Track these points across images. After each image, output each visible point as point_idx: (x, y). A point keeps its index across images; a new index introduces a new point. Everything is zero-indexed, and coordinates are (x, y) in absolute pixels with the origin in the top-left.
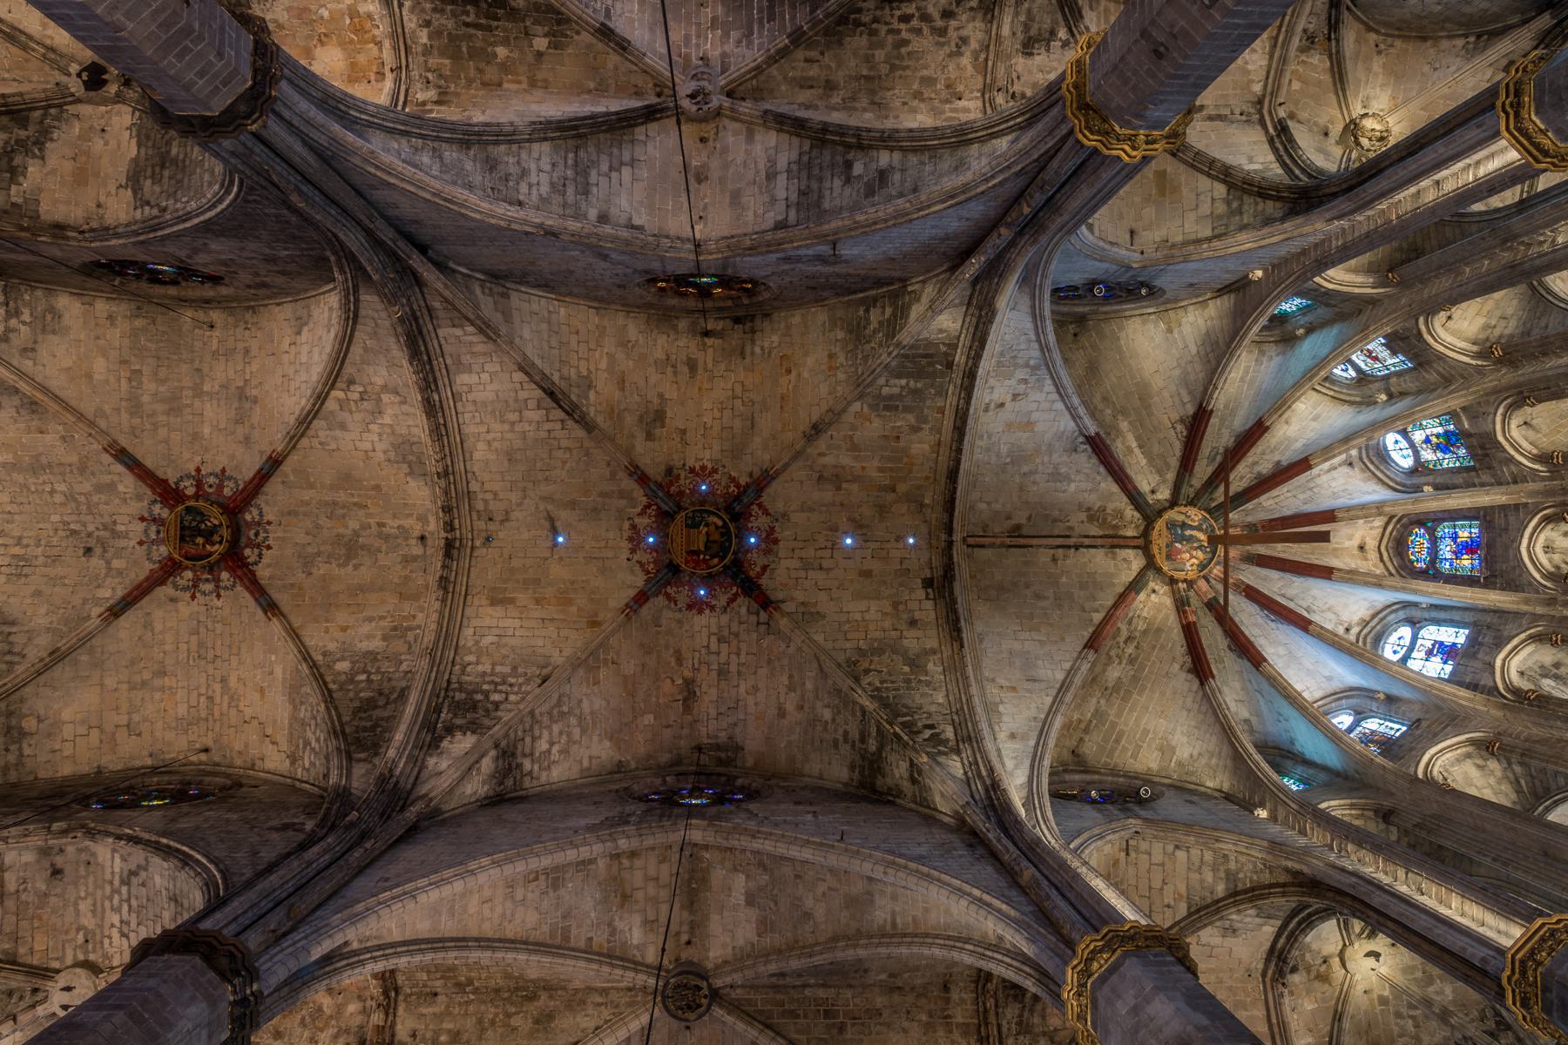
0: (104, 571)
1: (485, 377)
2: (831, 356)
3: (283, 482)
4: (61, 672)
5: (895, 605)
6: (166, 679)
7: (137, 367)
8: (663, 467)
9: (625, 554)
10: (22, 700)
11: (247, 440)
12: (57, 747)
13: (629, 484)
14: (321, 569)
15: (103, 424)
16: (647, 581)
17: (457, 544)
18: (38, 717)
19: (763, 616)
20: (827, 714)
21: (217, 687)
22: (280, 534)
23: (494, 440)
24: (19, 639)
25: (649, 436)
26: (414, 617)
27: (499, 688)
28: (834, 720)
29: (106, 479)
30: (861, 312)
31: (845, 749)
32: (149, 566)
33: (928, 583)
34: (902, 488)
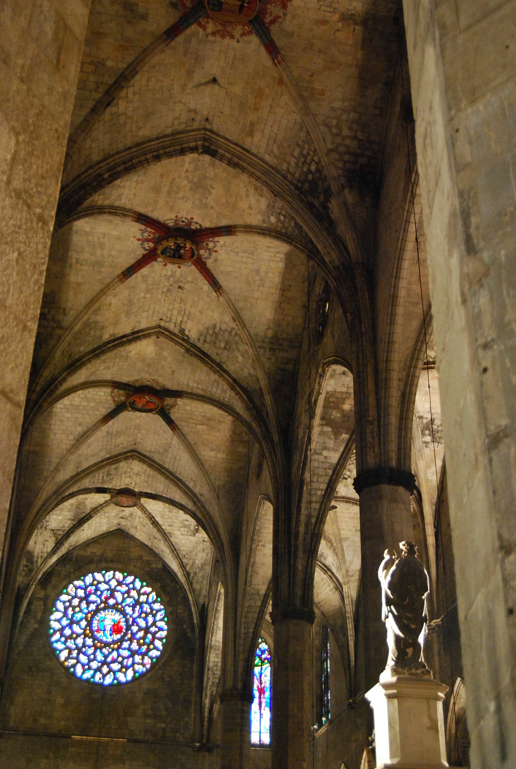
0: (193, 285)
1: (93, 145)
3: (152, 212)
4: (246, 315)
6: (261, 270)
7: (74, 260)
8: (170, 10)
9: (234, 43)
10: (257, 335)
12: (286, 323)
13: (180, 39)
15: (107, 281)
17: (207, 144)
18: (268, 329)
22: (185, 212)
23: (137, 126)
24: (224, 327)
25: (144, 17)
27: (308, 161)
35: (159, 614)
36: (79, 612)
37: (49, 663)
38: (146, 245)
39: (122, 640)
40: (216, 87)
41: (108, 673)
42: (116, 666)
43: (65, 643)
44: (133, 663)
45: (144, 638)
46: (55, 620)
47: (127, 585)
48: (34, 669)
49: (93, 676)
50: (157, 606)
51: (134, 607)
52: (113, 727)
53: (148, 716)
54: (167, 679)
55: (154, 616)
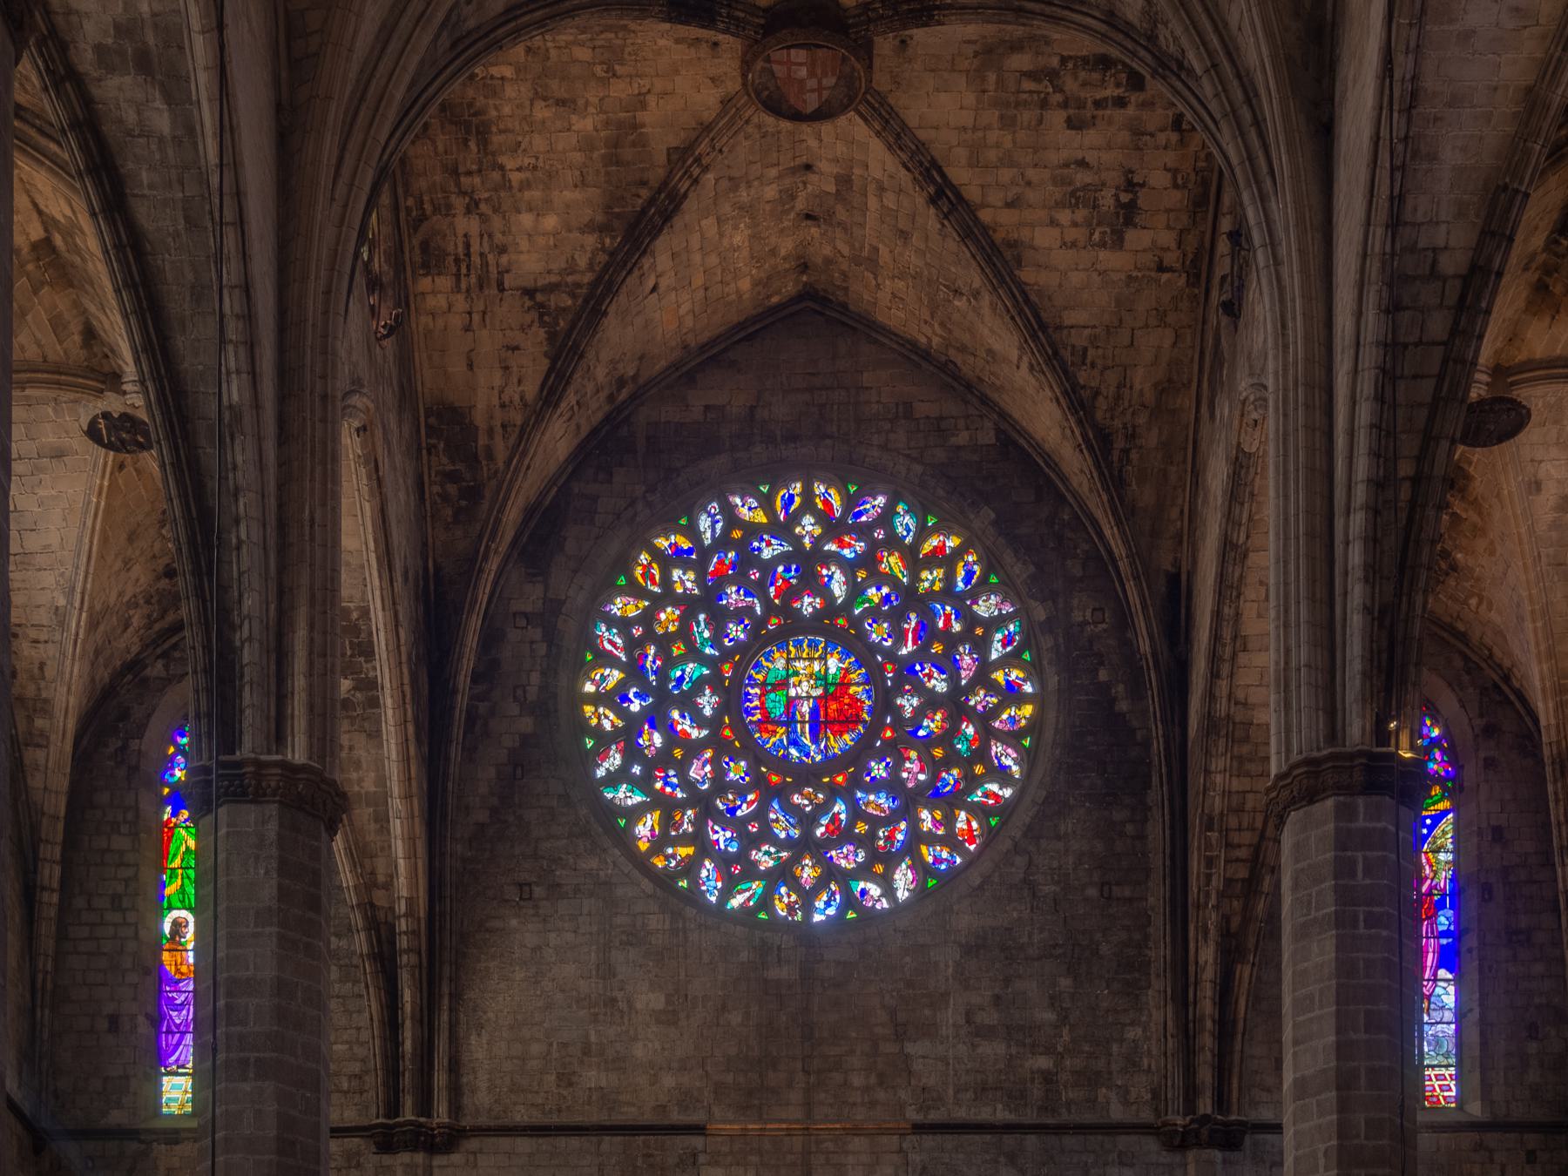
35: (999, 636)
36: (683, 659)
37: (593, 863)
39: (857, 758)
41: (821, 884)
42: (846, 858)
43: (643, 784)
44: (917, 837)
45: (949, 735)
46: (597, 699)
47: (863, 532)
48: (538, 891)
49: (765, 902)
50: (985, 607)
51: (897, 617)
52: (857, 1080)
53: (985, 1033)
54: (1048, 889)
55: (982, 646)
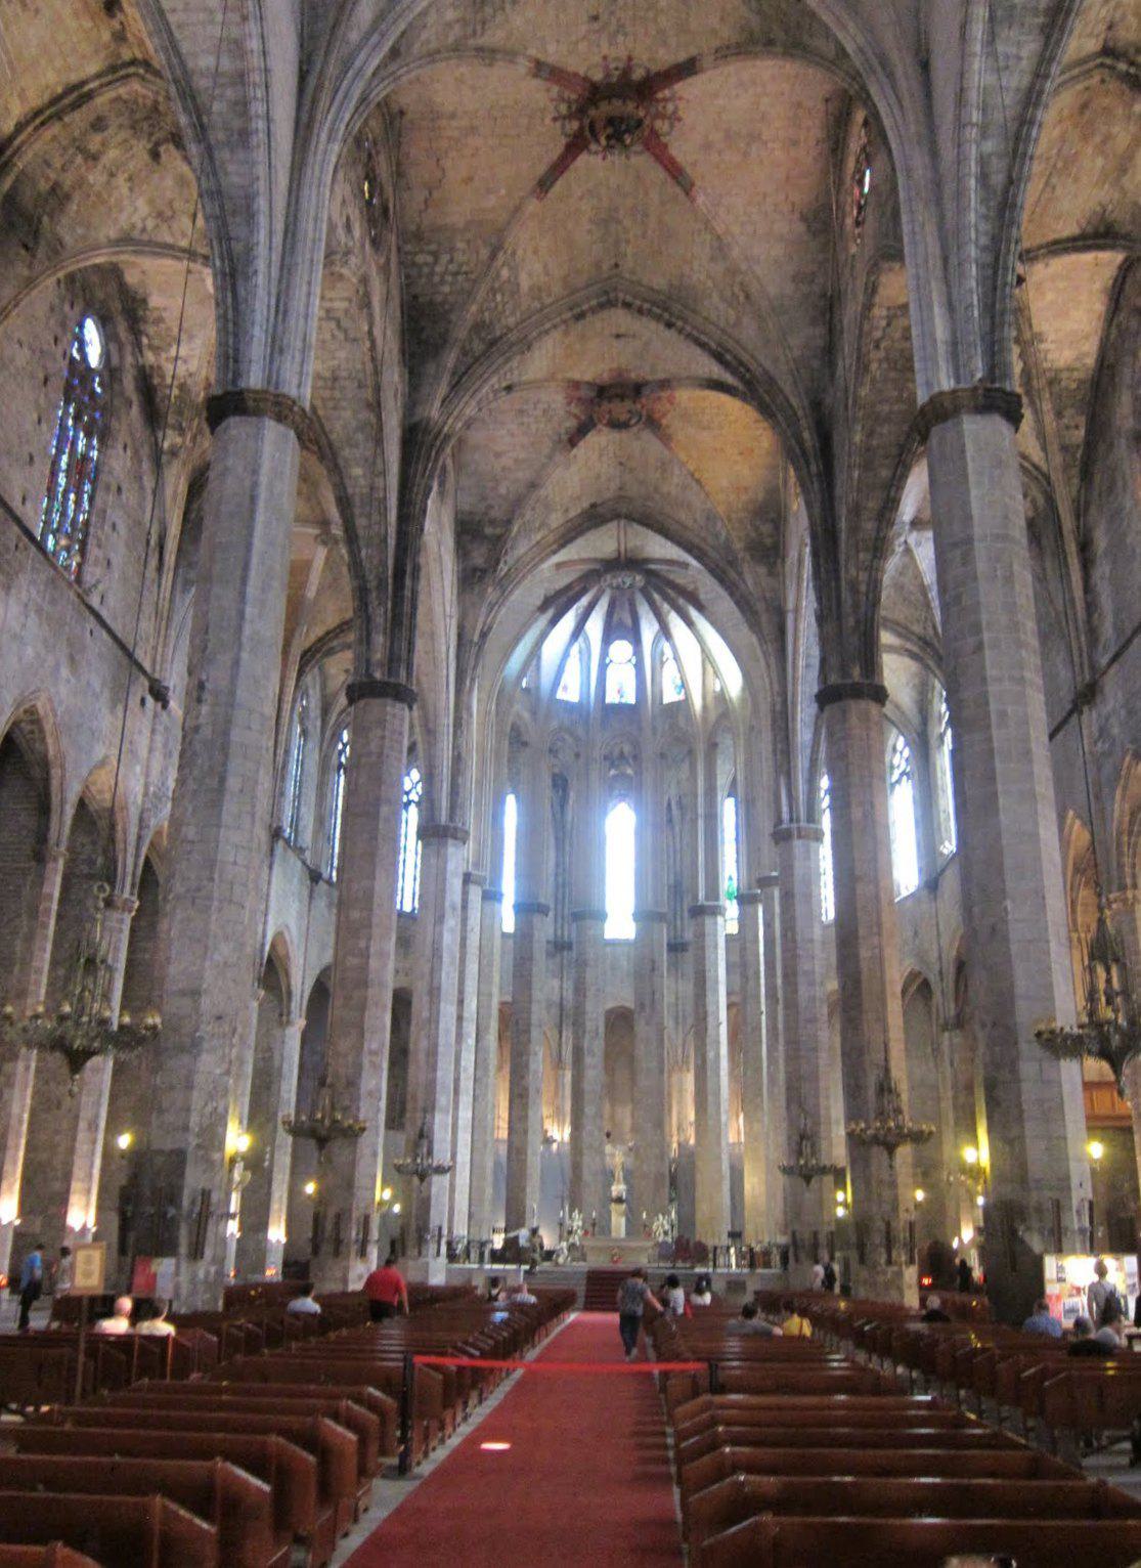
2: (746, 489)
5: (579, 498)
11: (707, 146)
14: (585, 206)
16: (588, 383)
19: (565, 438)
20: (503, 490)
21: (464, 122)
24: (499, 18)
26: (549, 295)
28: (500, 496)
29: (673, 41)
30: (772, 515)
31: (482, 507)
32: (582, 73)
33: (593, 506)
34: (657, 497)
38: (667, 93)
40: (614, 332)
